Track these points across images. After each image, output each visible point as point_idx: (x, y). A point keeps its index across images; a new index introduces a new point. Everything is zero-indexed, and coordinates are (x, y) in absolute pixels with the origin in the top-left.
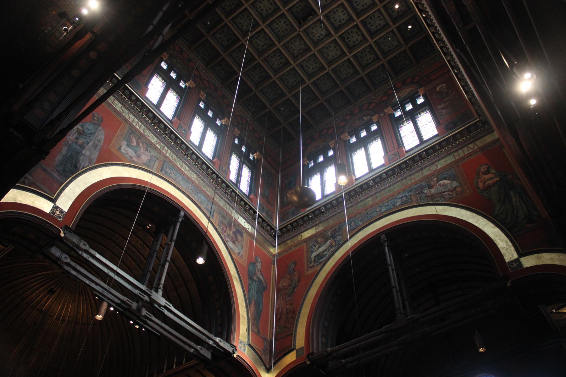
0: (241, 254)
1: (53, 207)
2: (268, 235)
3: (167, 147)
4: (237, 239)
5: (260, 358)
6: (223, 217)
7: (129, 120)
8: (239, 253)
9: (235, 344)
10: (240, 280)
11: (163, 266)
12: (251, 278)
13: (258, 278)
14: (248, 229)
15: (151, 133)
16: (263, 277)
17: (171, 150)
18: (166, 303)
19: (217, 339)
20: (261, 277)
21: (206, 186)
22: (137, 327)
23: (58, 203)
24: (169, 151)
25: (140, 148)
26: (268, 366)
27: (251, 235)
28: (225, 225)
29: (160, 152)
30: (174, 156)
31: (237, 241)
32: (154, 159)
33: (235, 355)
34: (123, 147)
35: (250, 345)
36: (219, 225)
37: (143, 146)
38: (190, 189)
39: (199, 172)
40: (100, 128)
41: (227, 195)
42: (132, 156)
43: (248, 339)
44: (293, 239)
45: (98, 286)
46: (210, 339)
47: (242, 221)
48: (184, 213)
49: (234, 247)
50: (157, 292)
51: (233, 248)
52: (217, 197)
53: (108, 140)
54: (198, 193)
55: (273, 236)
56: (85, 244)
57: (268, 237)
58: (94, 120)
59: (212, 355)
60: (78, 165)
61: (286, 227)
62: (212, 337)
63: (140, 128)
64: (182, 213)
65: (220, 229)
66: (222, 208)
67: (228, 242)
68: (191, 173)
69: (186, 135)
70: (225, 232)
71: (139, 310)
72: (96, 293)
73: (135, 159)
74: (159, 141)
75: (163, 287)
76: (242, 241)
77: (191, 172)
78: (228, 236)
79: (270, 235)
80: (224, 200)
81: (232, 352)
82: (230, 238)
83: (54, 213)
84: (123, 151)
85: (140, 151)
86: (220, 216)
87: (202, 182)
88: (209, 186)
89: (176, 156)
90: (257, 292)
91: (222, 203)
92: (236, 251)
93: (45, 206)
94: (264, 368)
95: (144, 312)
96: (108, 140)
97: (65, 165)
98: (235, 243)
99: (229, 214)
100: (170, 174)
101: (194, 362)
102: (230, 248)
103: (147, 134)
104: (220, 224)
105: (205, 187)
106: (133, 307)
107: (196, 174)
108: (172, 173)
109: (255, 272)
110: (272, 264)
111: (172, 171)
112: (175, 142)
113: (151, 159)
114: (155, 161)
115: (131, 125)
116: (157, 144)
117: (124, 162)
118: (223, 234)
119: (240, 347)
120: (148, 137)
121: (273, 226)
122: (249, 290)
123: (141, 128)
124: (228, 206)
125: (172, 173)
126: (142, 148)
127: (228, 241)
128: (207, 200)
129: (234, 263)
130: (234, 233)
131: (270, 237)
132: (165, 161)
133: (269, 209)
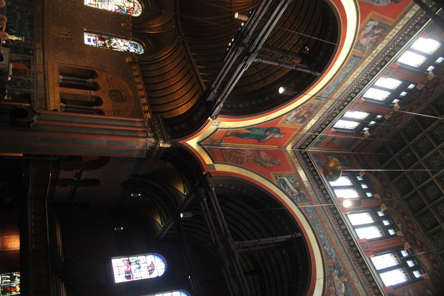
0: (287, 122)
2: (302, 143)
3: (373, 59)
4: (297, 119)
5: (208, 137)
6: (316, 107)
7: (397, 26)
8: (287, 120)
9: (218, 118)
10: (266, 122)
11: (276, 61)
12: (267, 130)
13: (268, 135)
14: (306, 127)
15: (385, 45)
16: (269, 139)
17: (371, 62)
18: (248, 65)
19: (221, 105)
21: (341, 93)
22: (230, 44)
24: (370, 61)
25: (372, 37)
26: (201, 143)
27: (301, 129)
28: (309, 109)
29: (369, 54)
30: (365, 66)
32: (363, 49)
33: (209, 118)
34: (373, 23)
35: (217, 130)
36: (309, 104)
37: (374, 39)
38: (338, 80)
39: (352, 87)
41: (333, 110)
42: (365, 30)
43: (222, 128)
44: (298, 162)
45: (259, 12)
46: (222, 99)
47: (313, 122)
48: (319, 75)
49: (292, 117)
50: (256, 58)
51: (291, 115)
52: (332, 102)
54: (335, 87)
55: (301, 147)
59: (210, 102)
61: (308, 157)
62: (223, 101)
63: (390, 35)
64: (318, 74)
65: (306, 105)
66: (323, 106)
67: (295, 112)
68: (351, 80)
69: (384, 74)
70: (304, 109)
71: (243, 45)
72: (254, 11)
73: (363, 33)
74: (379, 52)
75: (260, 62)
76: (297, 122)
77: (353, 80)
78: (301, 112)
79: (301, 145)
80: (329, 108)
81: (212, 116)
82: (299, 113)
84: (370, 22)
85: (370, 37)
86: (317, 105)
87: (344, 89)
88: (341, 95)
89: (366, 67)
90: (257, 134)
91: (327, 106)
92: (289, 118)
94: (200, 140)
95: (241, 49)
96: (378, 9)
98: (295, 117)
99: (318, 112)
100: (350, 63)
101: (205, 88)
102: (291, 113)
103: (385, 42)
104: (310, 105)
105: (340, 92)
106: (244, 40)
107: (351, 84)
108: (351, 65)
109: (273, 133)
110: (279, 146)
111: (353, 64)
112: (378, 66)
113: (363, 46)
114: (361, 50)
116: (376, 50)
117: (361, 23)
118: (302, 107)
119: (215, 122)
120: (382, 43)
121: (309, 147)
122: (258, 128)
123: (390, 36)
124: (324, 111)
125: (351, 65)
126: (373, 39)
127: (296, 112)
128: (329, 93)
129: (279, 116)
130: (303, 116)
131: (300, 145)
132: (361, 58)
133: (323, 144)
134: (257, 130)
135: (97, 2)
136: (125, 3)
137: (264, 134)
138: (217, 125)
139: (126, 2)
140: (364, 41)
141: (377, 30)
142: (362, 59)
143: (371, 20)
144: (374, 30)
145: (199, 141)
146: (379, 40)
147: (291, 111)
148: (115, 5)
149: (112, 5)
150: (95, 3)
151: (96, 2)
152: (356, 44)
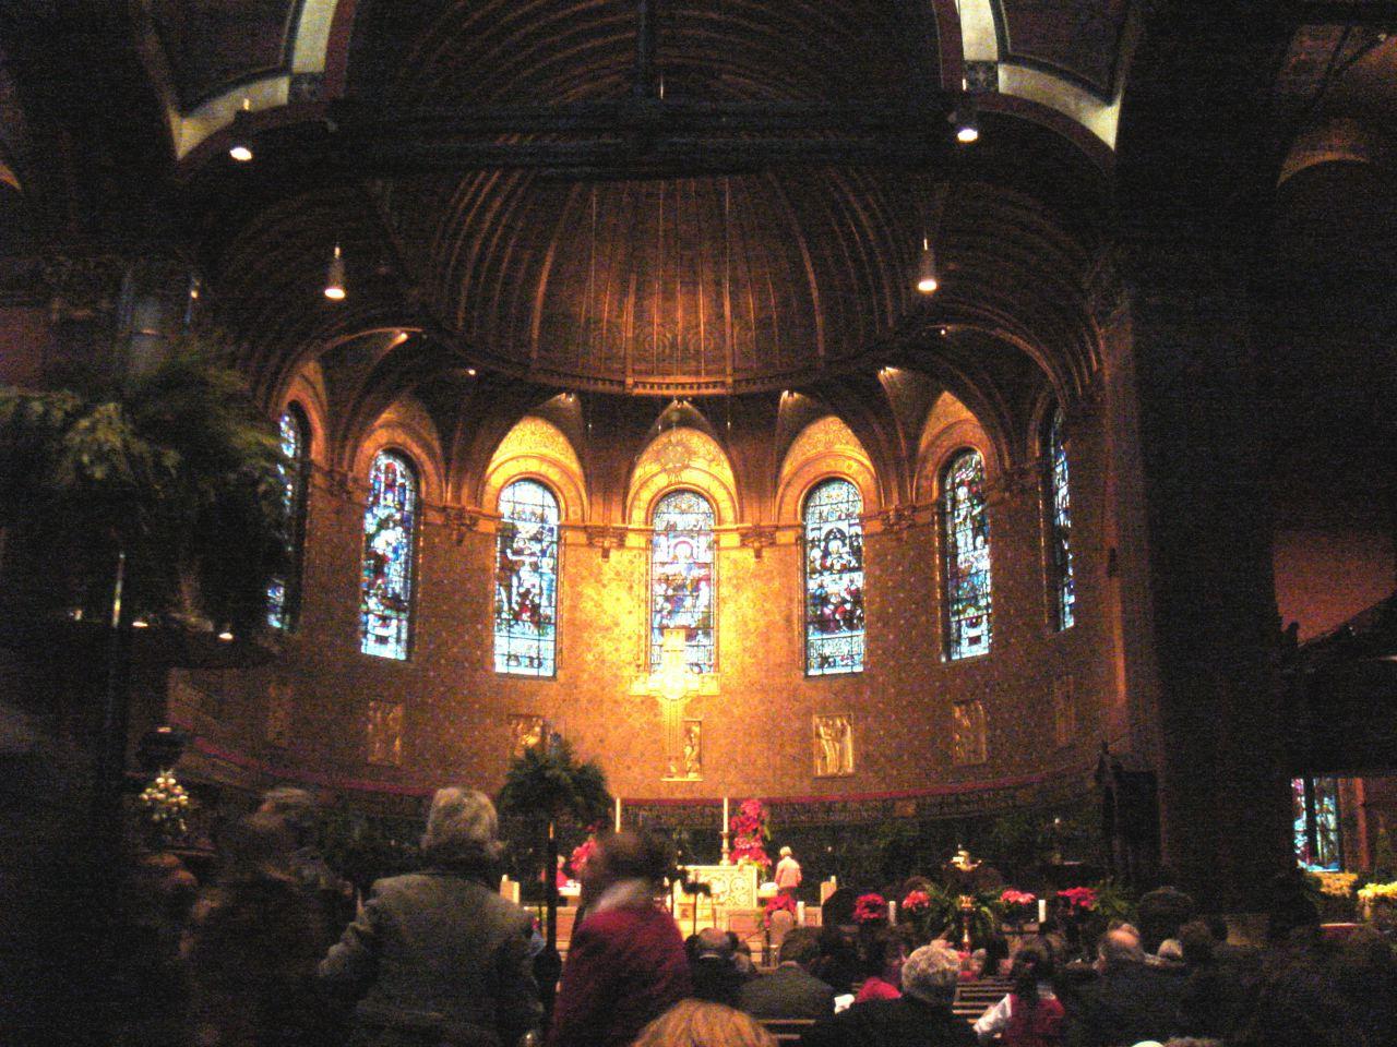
1: (292, 84)
135: (980, 613)
136: (961, 519)
139: (959, 515)
148: (975, 548)
149: (976, 559)
150: (985, 617)
151: (981, 617)
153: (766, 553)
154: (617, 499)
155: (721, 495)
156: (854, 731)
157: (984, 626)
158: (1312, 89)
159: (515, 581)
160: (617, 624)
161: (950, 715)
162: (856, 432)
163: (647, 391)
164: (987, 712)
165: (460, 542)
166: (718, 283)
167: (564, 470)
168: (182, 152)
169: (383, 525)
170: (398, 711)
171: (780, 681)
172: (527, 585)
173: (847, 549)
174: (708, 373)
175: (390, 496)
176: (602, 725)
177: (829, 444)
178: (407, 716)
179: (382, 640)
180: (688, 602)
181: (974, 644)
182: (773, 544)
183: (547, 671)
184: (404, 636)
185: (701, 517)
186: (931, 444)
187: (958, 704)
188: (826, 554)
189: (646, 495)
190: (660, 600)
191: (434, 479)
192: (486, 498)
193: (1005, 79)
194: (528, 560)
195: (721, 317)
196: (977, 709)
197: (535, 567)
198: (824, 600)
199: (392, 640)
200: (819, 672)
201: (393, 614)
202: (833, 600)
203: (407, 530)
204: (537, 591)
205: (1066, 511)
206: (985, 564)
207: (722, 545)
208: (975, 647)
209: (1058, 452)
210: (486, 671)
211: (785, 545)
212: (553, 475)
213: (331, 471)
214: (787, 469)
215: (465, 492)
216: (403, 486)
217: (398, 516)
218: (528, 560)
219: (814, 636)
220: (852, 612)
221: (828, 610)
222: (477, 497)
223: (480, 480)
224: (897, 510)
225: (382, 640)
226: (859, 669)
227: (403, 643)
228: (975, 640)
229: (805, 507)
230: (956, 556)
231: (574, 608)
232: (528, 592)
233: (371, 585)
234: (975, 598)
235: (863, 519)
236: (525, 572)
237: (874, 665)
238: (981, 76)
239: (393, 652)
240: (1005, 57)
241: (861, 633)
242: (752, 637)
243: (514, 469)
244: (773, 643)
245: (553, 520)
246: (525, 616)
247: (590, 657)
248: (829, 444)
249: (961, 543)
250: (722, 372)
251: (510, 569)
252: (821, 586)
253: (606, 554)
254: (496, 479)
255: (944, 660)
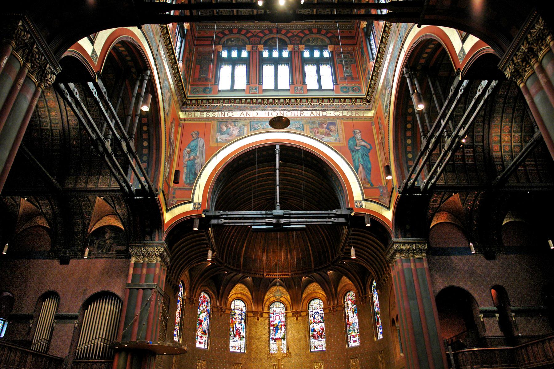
4: (331, 131)
16: (365, 142)
20: (364, 143)
23: (195, 200)
31: (331, 131)
32: (242, 127)
40: (199, 139)
53: (207, 141)
56: (219, 212)
57: (362, 107)
58: (193, 137)
60: (196, 172)
64: (277, 147)
70: (318, 133)
73: (229, 139)
76: (335, 129)
78: (322, 133)
83: (195, 208)
93: (189, 207)
94: (385, 209)
96: (207, 141)
97: (189, 177)
115: (218, 119)
118: (315, 136)
130: (327, 128)
134: (356, 160)
137: (360, 151)
138: (360, 202)
140: (235, 132)
141: (223, 129)
142: (251, 120)
143: (217, 141)
144: (224, 132)
145: (386, 209)
146: (231, 121)
147: (324, 144)
152: (241, 137)
153: (299, 318)
154: (261, 304)
155: (287, 303)
156: (324, 366)
157: (357, 338)
158: (437, 206)
159: (235, 327)
160: (261, 338)
161: (349, 362)
162: (321, 287)
163: (269, 277)
164: (359, 361)
165: (221, 316)
166: (287, 250)
167: (247, 297)
168: (166, 221)
169: (201, 312)
170: (205, 363)
171: (303, 352)
172: (238, 327)
173: (320, 317)
174: (284, 272)
175: (204, 304)
176: (257, 366)
177: (314, 290)
178: (207, 364)
179: (201, 343)
180: (279, 331)
181: (354, 342)
182: (301, 316)
183: (243, 351)
184: (206, 342)
185: (282, 309)
186: (340, 290)
187: (352, 359)
188: (314, 318)
189: (268, 303)
190: (272, 331)
191: (215, 299)
192: (228, 304)
193: (365, 205)
194: (238, 320)
195: (287, 258)
196: (357, 360)
197: (240, 323)
198: (314, 331)
199: (203, 343)
200: (314, 350)
201: (204, 336)
202: (317, 331)
203: (208, 313)
204: (240, 329)
205: (378, 307)
206: (357, 321)
207: (288, 316)
208: (355, 343)
209: (374, 292)
210: (227, 351)
211: (304, 316)
212: (244, 298)
213: (190, 298)
214: (304, 296)
215: (223, 303)
216: (207, 301)
217: (206, 309)
218: (238, 320)
219: (312, 340)
220: (322, 334)
221: (315, 333)
222: (225, 304)
223: (227, 299)
224: (333, 307)
225: (201, 343)
226: (324, 349)
227: (206, 344)
228: (355, 341)
229: (308, 306)
230: (348, 319)
231: (250, 333)
232: (238, 329)
233: (199, 328)
234: (354, 330)
235: (324, 309)
236: (237, 324)
237: (328, 348)
238: (359, 204)
239: (203, 346)
240: (365, 200)
241: (324, 340)
242: (296, 341)
243: (234, 296)
244: (301, 343)
245: (244, 310)
246: (237, 336)
247: (254, 347)
248: (314, 290)
249: (349, 315)
250: (288, 272)
251: (233, 322)
252: (313, 327)
253: (258, 319)
254: (230, 299)
255: (347, 346)
